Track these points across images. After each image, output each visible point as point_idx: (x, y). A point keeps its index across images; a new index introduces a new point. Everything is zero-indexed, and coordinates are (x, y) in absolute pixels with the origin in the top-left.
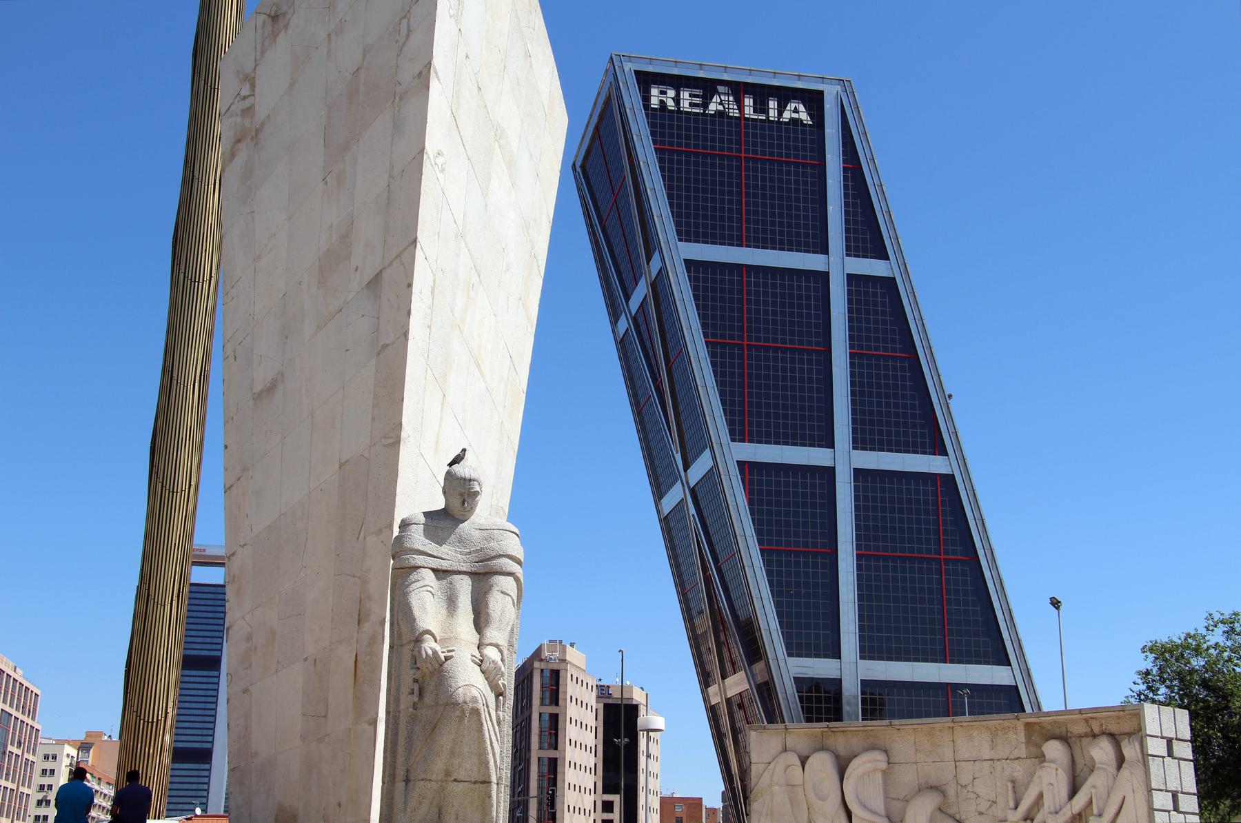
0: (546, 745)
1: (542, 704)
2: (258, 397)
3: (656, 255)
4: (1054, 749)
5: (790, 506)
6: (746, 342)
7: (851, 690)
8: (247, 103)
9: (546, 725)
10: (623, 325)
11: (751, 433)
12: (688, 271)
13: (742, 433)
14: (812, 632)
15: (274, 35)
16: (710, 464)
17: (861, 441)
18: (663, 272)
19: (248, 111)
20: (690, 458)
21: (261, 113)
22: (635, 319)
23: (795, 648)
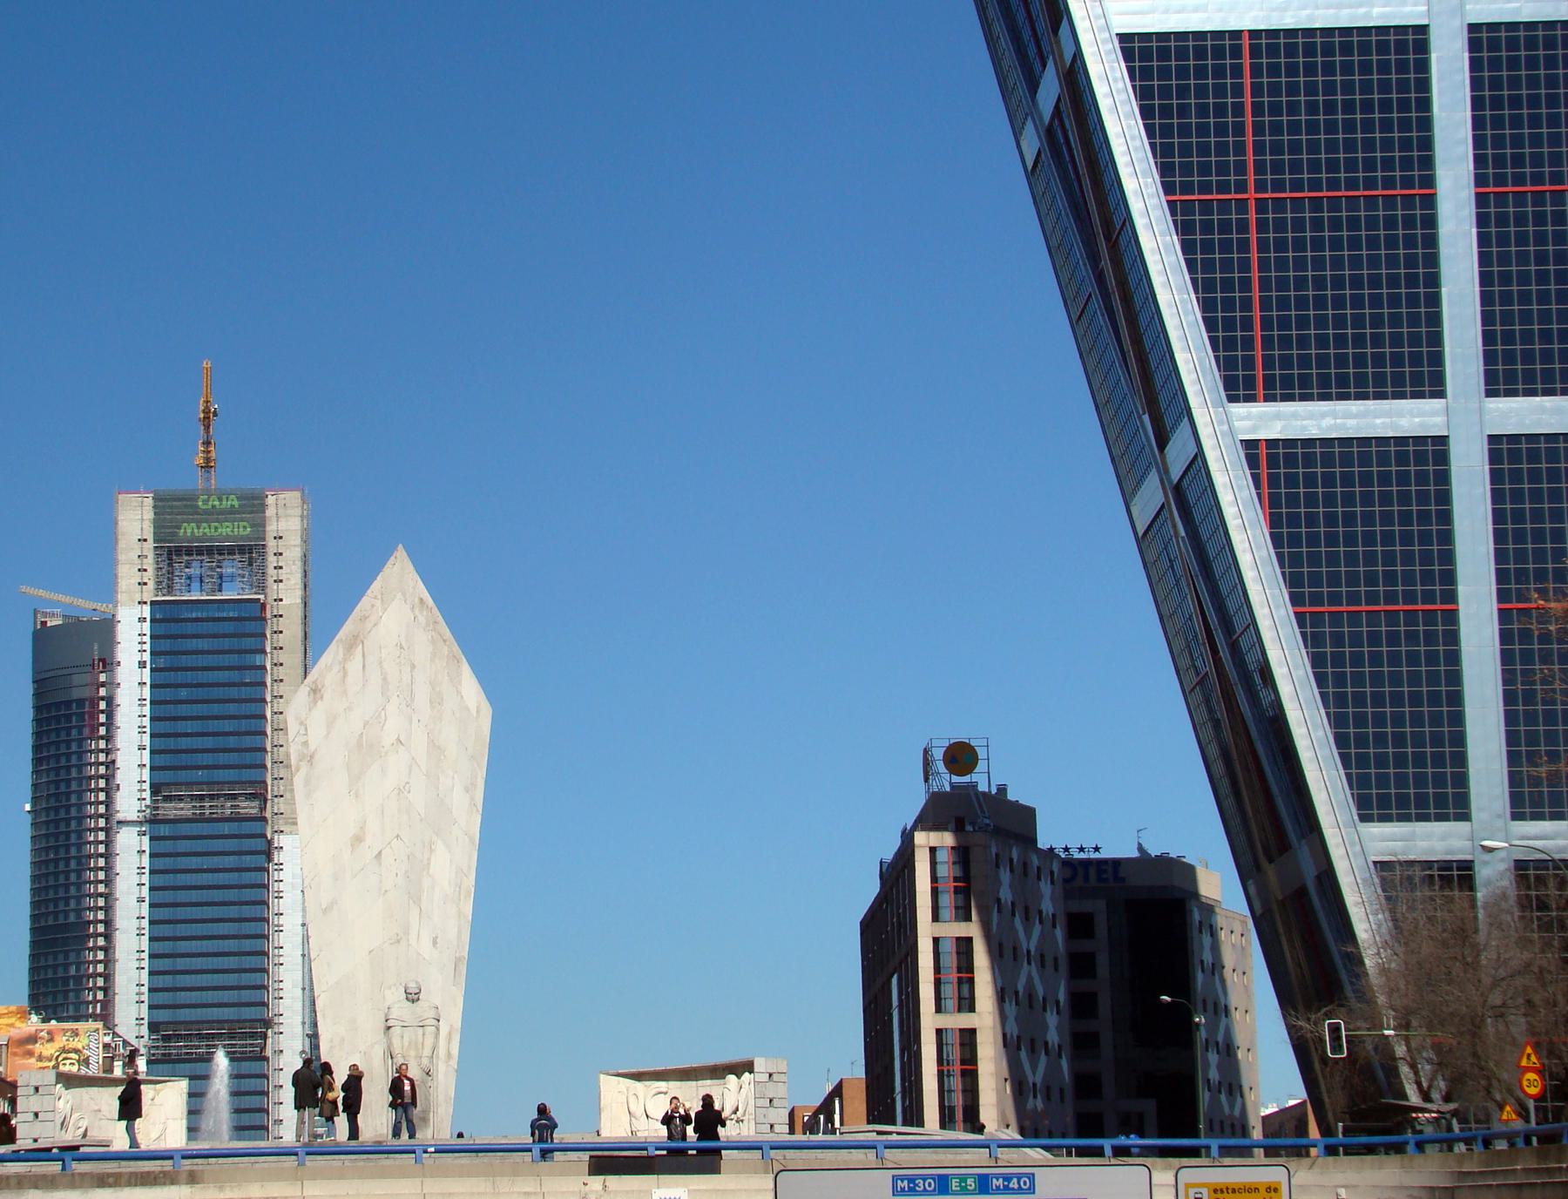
0: (950, 1004)
1: (936, 918)
2: (325, 911)
3: (1065, 22)
4: (732, 1078)
5: (1361, 521)
6: (1251, 194)
7: (1492, 876)
8: (303, 739)
9: (950, 960)
10: (1032, 143)
11: (1269, 382)
12: (1128, 55)
13: (1250, 382)
14: (1408, 766)
15: (315, 702)
16: (1193, 450)
17: (1498, 382)
18: (1078, 55)
19: (306, 744)
20: (1168, 422)
21: (312, 748)
22: (1049, 132)
23: (1373, 803)
